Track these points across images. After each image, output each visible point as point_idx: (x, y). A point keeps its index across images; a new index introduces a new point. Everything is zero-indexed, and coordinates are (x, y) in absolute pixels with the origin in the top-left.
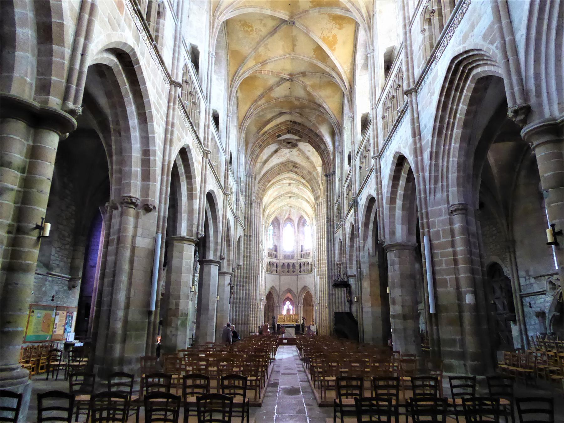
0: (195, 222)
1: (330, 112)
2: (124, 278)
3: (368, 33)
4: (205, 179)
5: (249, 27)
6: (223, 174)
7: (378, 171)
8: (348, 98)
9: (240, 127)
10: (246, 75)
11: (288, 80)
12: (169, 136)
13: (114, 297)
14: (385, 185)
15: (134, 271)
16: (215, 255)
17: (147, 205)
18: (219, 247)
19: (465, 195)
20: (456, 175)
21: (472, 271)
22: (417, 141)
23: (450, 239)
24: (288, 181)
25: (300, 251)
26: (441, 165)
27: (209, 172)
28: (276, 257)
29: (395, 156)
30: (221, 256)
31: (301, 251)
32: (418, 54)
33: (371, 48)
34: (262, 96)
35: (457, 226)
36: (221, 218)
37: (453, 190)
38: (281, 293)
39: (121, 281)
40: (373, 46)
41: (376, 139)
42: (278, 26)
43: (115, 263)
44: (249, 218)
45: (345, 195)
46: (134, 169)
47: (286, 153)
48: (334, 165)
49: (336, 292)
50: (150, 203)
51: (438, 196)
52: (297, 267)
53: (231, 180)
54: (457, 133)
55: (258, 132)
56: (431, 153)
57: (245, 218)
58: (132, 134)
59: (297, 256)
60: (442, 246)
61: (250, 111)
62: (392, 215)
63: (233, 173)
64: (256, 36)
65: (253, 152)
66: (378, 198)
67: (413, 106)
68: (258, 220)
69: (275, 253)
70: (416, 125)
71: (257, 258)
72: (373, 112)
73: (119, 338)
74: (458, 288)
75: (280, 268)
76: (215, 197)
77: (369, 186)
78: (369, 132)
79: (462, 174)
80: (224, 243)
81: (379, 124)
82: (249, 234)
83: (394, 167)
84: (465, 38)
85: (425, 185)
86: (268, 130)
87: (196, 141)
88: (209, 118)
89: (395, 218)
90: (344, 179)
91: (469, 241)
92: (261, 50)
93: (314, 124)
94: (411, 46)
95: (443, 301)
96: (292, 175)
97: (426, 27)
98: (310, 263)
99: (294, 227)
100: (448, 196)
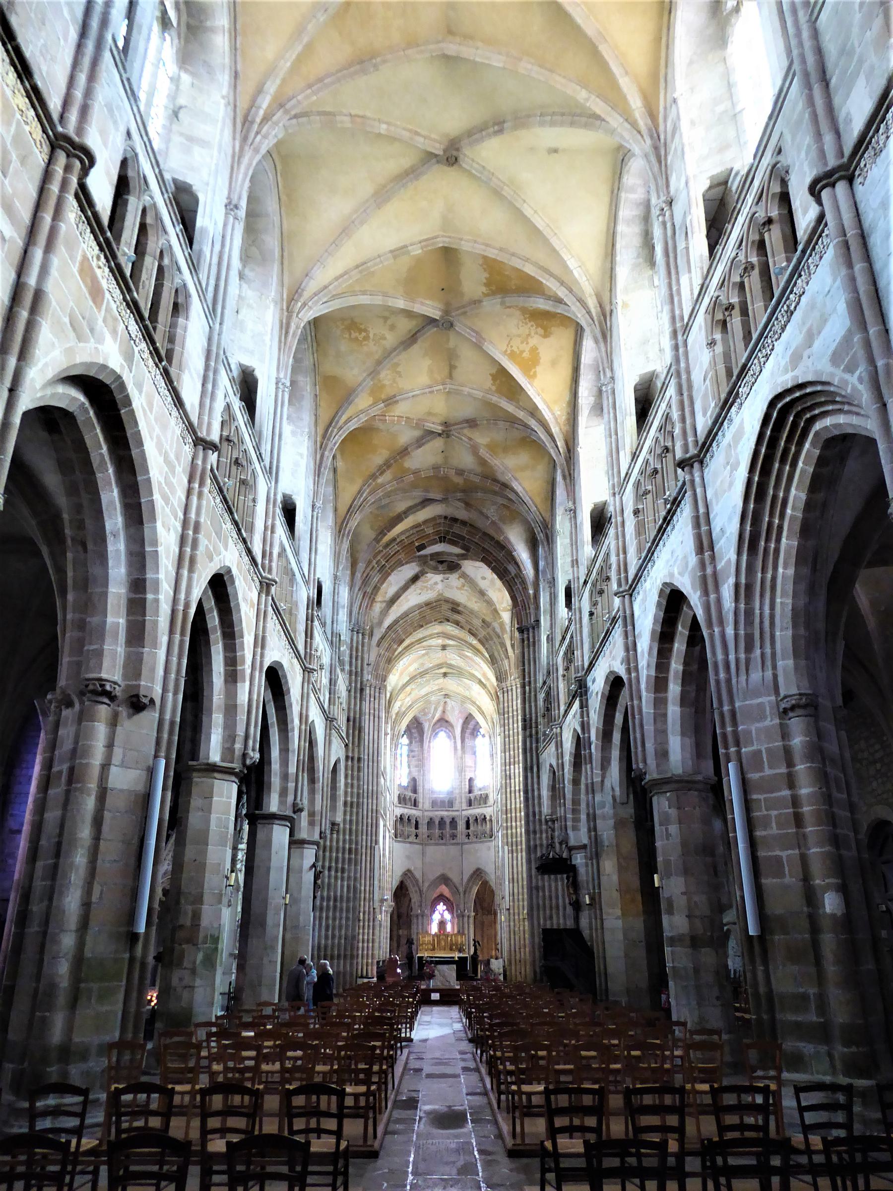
0: (240, 731)
1: (527, 499)
2: (80, 859)
3: (602, 345)
4: (264, 638)
5: (360, 331)
6: (301, 627)
7: (629, 621)
8: (563, 471)
9: (340, 529)
10: (353, 426)
11: (440, 435)
12: (188, 550)
13: (55, 903)
14: (643, 652)
15: (101, 841)
16: (282, 802)
17: (137, 696)
18: (291, 785)
19: (812, 678)
20: (790, 633)
21: (835, 841)
22: (707, 562)
23: (783, 770)
24: (440, 641)
25: (467, 790)
26: (757, 612)
27: (272, 624)
28: (415, 804)
29: (661, 590)
30: (294, 805)
31: (470, 792)
32: (703, 388)
33: (609, 374)
34: (387, 465)
35: (798, 741)
36: (296, 721)
37: (786, 664)
38: (426, 884)
39: (72, 864)
40: (612, 370)
41: (621, 556)
42: (418, 331)
43: (62, 826)
44: (357, 720)
45: (561, 672)
46: (110, 619)
47: (436, 583)
48: (537, 607)
49: (546, 884)
50: (142, 692)
51: (756, 676)
52: (461, 825)
53: (320, 641)
54: (789, 547)
55: (377, 540)
56: (737, 586)
57: (348, 720)
58: (111, 548)
60: (769, 786)
61: (361, 496)
62: (660, 716)
63: (323, 625)
64: (373, 349)
65: (365, 581)
66: (630, 680)
67: (695, 491)
68: (376, 724)
69: (413, 796)
70: (704, 528)
71: (374, 808)
72: (615, 500)
73: (62, 999)
74: (806, 878)
75: (423, 829)
76: (285, 677)
77: (611, 653)
78: (607, 542)
79: (802, 631)
80: (303, 776)
81: (627, 524)
82: (356, 756)
83: (662, 614)
84: (796, 359)
85: (726, 654)
86: (398, 536)
87: (246, 559)
88: (274, 512)
89: (665, 722)
90: (559, 638)
91: (826, 774)
92: (386, 375)
93: (493, 523)
94: (688, 373)
95: (775, 908)
96: (449, 628)
97: (718, 336)
98: (488, 818)
99: (455, 738)
100: (775, 676)
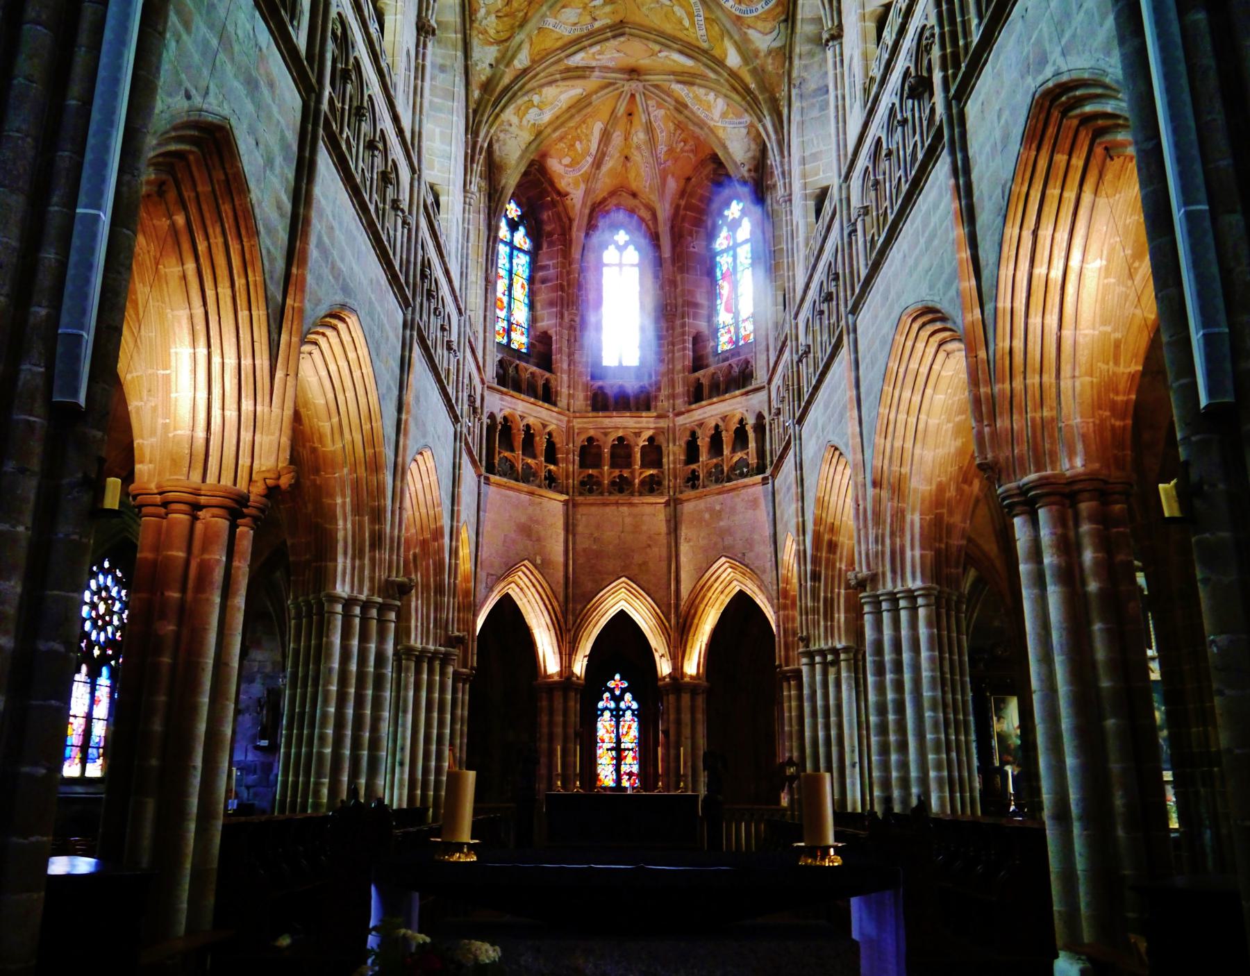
31: (698, 363)
52: (674, 453)
59: (673, 396)
